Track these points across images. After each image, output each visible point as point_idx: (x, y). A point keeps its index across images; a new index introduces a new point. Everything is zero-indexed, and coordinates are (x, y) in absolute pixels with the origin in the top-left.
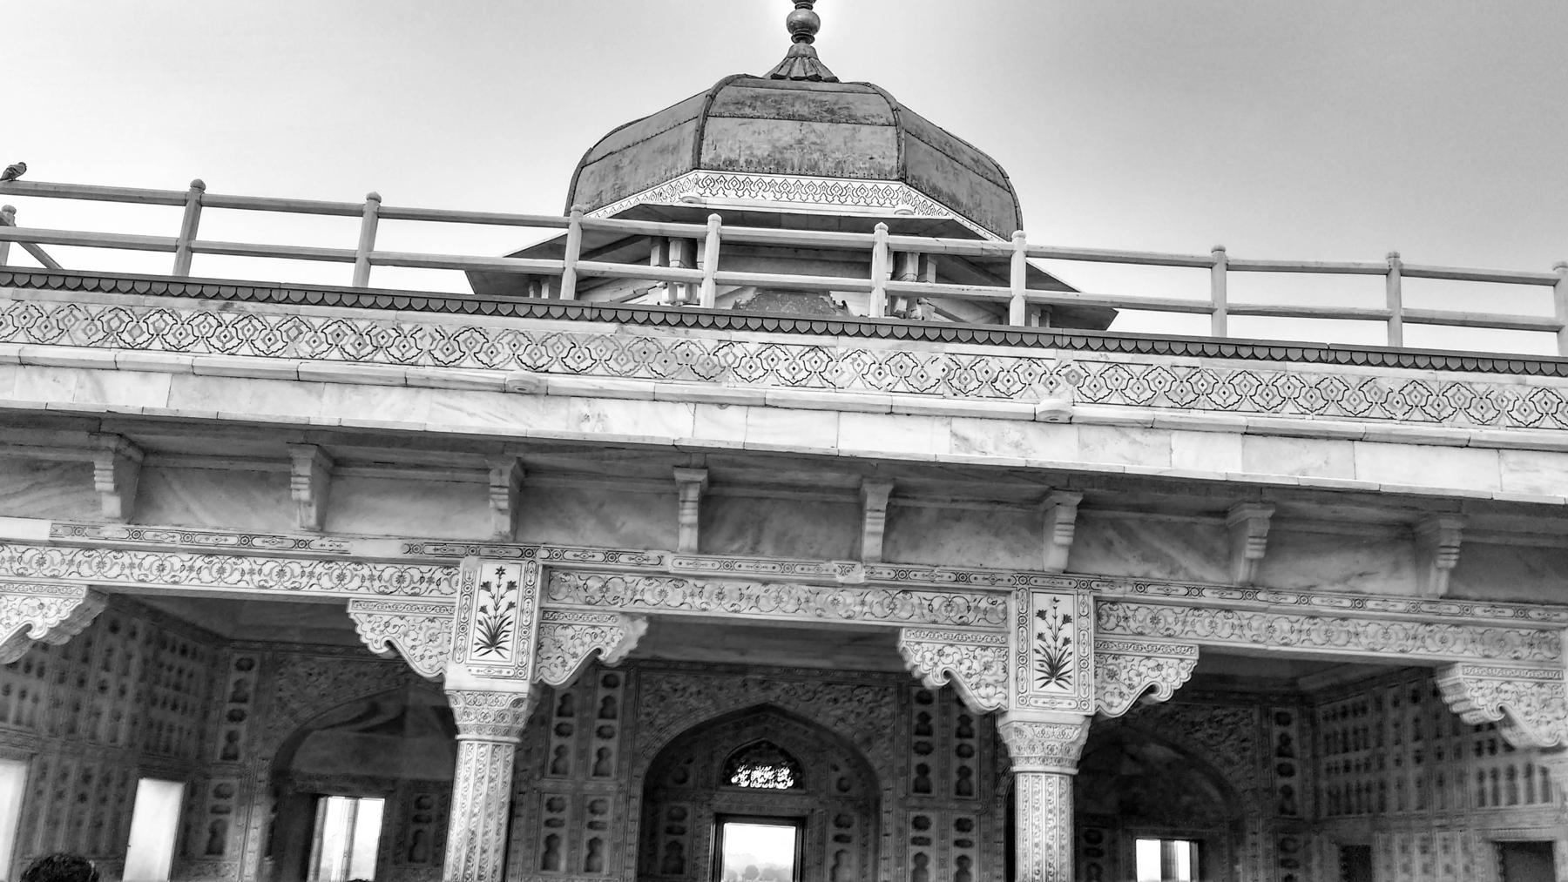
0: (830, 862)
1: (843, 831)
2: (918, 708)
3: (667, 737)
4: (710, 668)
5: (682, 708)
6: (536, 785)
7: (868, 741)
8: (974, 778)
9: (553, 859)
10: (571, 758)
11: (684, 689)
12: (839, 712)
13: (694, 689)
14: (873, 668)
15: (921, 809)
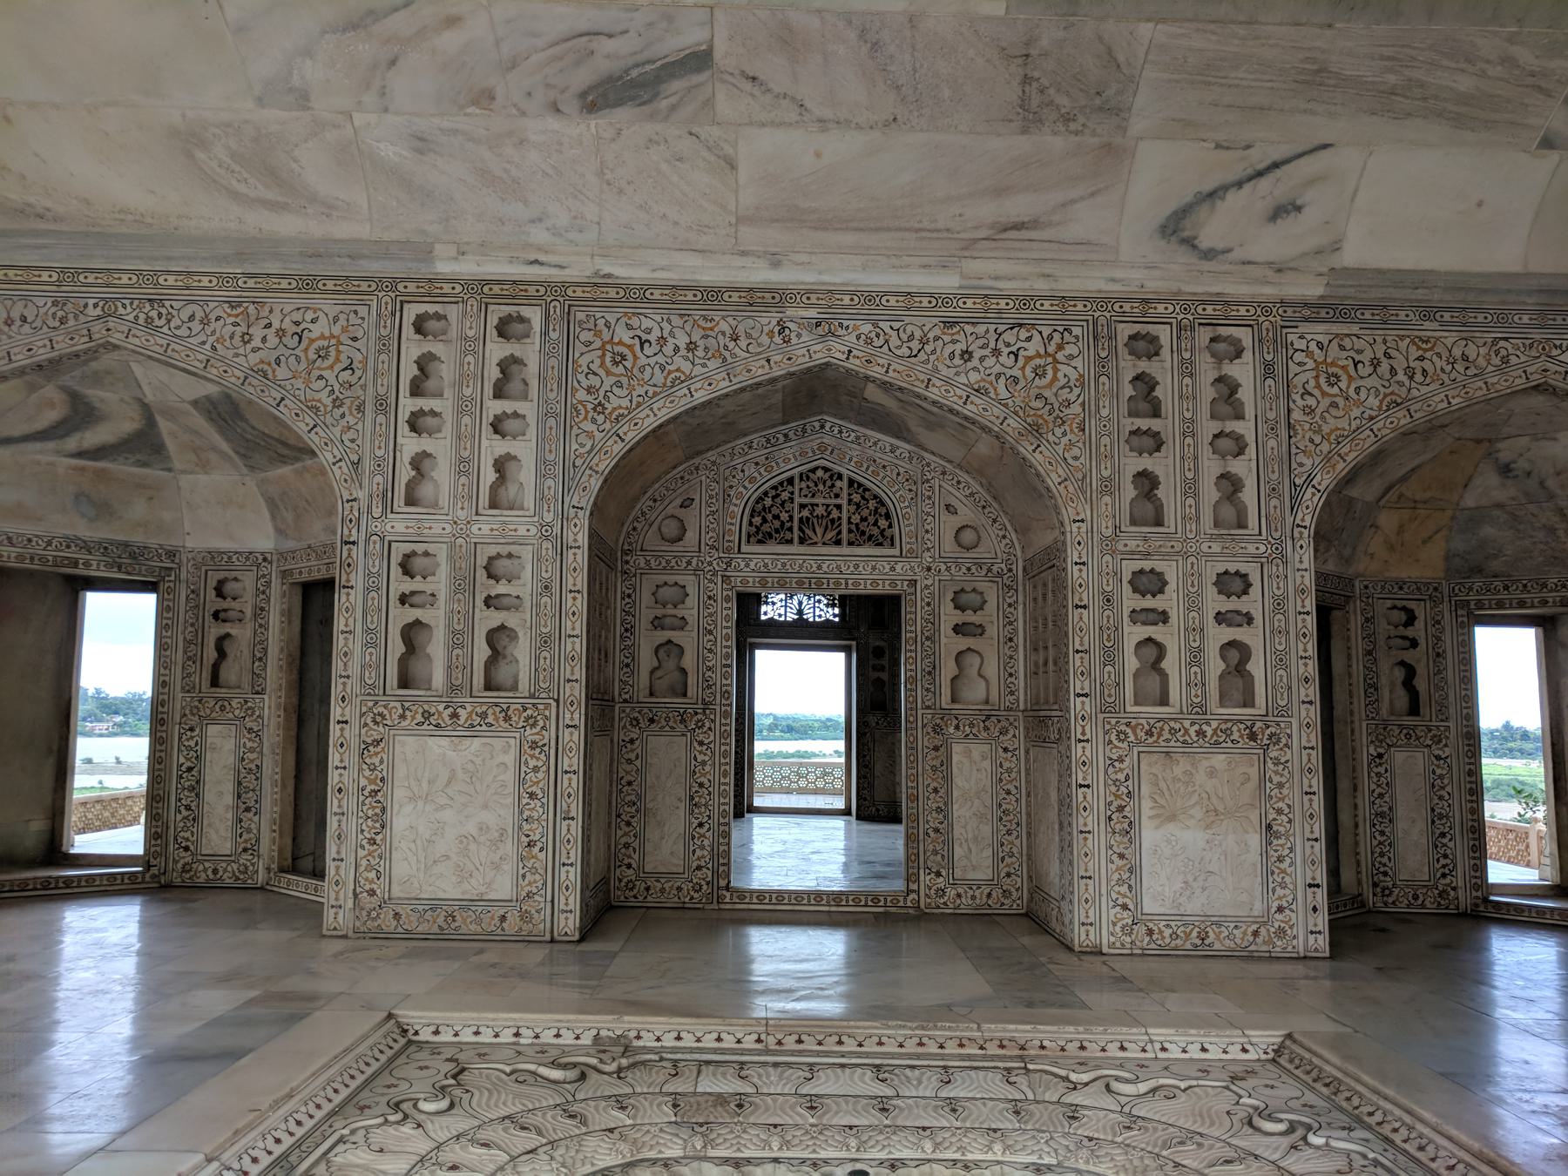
0: (948, 669)
1: (970, 617)
2: (1129, 367)
3: (632, 435)
4: (712, 295)
5: (659, 378)
6: (376, 526)
7: (1035, 430)
8: (1248, 496)
9: (417, 667)
10: (442, 474)
11: (662, 340)
12: (974, 376)
13: (682, 340)
14: (1042, 286)
15: (1147, 555)
